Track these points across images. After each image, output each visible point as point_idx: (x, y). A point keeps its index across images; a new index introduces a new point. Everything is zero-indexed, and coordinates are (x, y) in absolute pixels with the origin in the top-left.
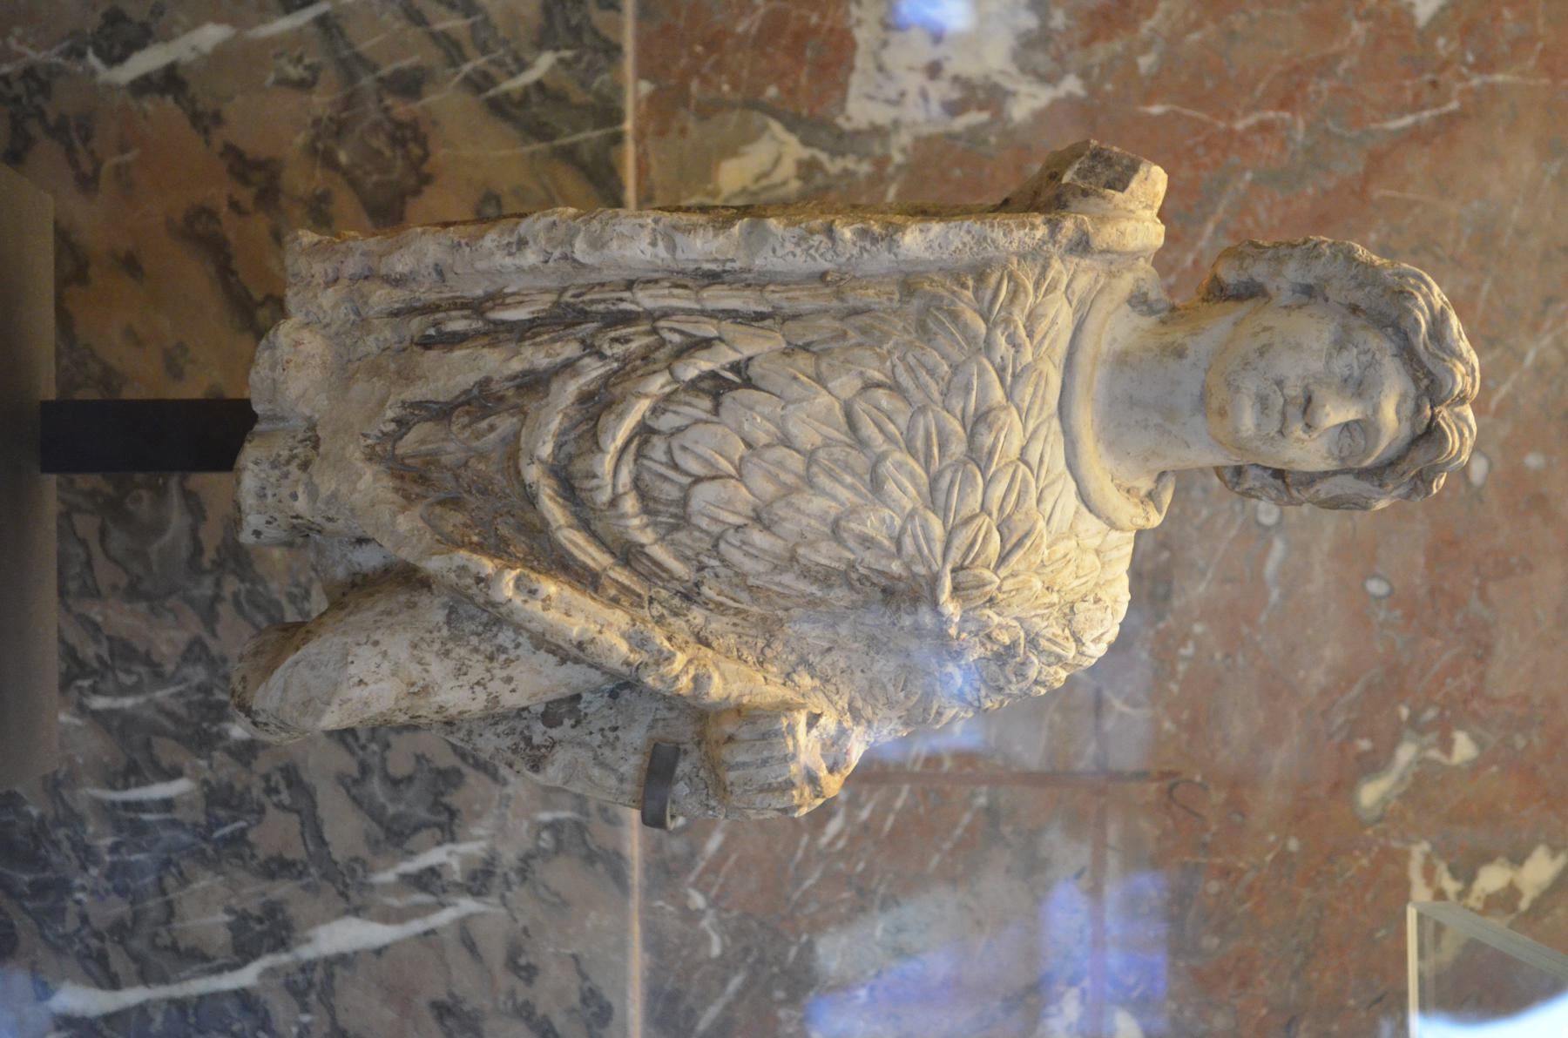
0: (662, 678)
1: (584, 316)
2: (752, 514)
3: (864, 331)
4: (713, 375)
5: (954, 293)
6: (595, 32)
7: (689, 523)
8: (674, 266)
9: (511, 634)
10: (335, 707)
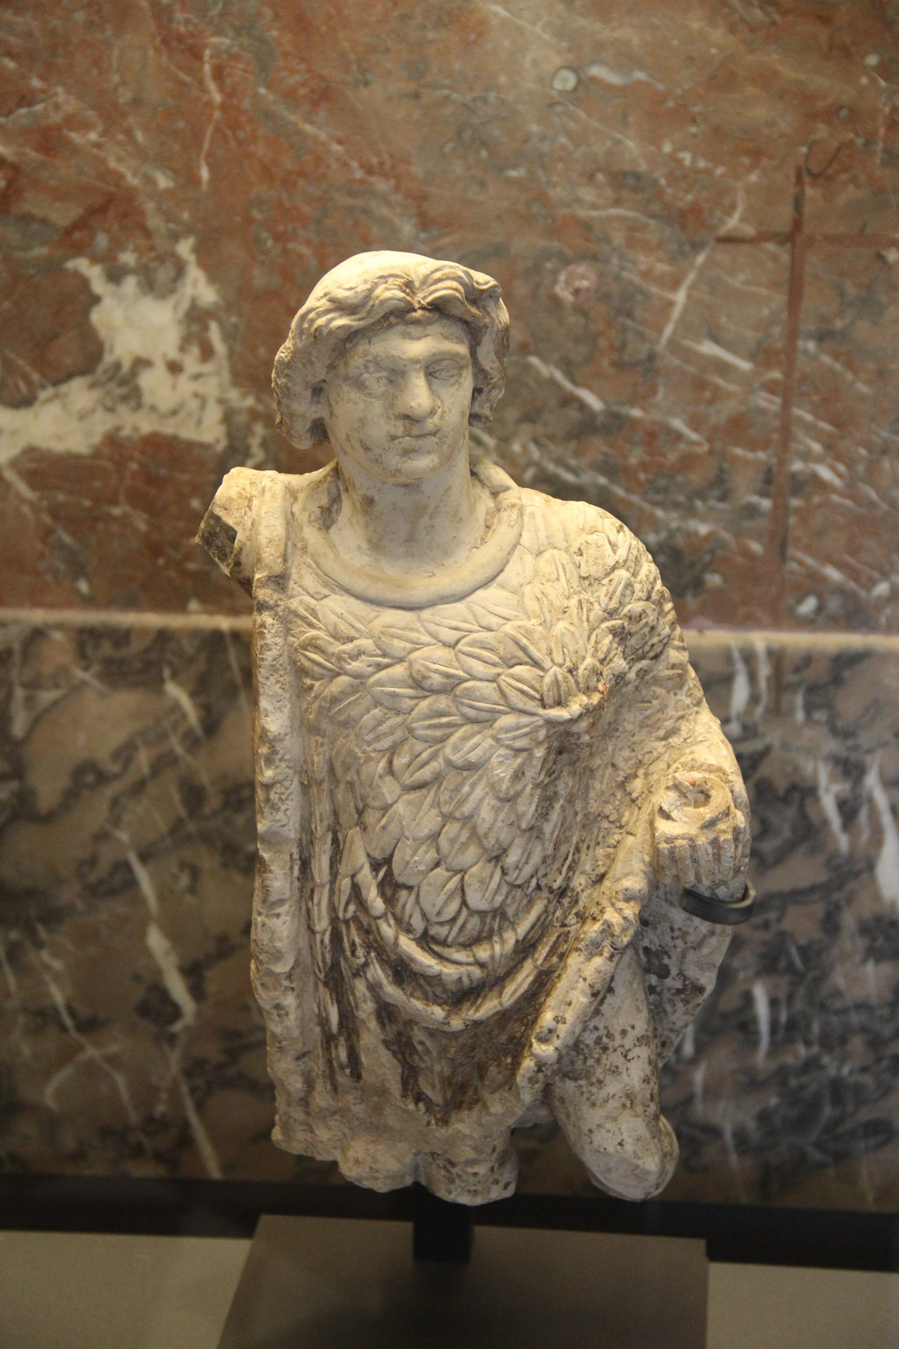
0: (624, 930)
1: (335, 965)
2: (493, 863)
3: (347, 768)
4: (381, 886)
5: (316, 697)
6: (147, 650)
7: (499, 908)
8: (295, 898)
9: (586, 1034)
10: (640, 1162)
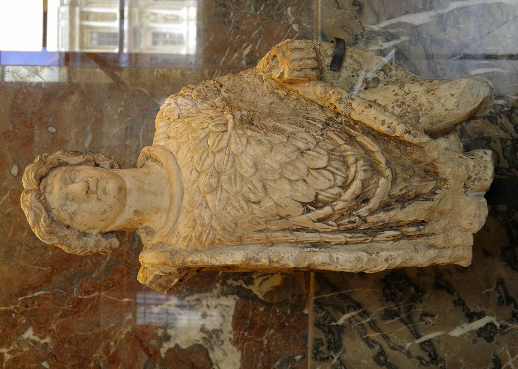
1: (364, 232)
2: (304, 155)
4: (317, 208)
6: (324, 332)
8: (330, 250)
9: (395, 112)
10: (462, 87)
